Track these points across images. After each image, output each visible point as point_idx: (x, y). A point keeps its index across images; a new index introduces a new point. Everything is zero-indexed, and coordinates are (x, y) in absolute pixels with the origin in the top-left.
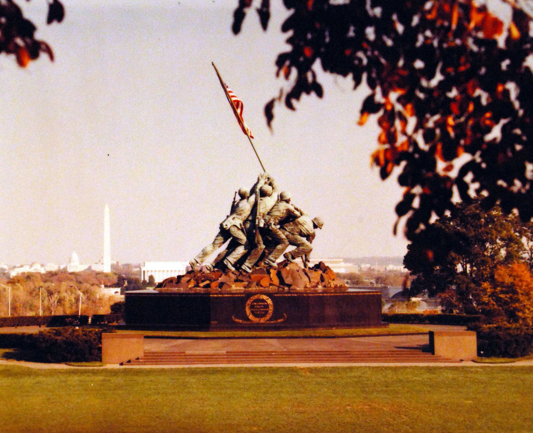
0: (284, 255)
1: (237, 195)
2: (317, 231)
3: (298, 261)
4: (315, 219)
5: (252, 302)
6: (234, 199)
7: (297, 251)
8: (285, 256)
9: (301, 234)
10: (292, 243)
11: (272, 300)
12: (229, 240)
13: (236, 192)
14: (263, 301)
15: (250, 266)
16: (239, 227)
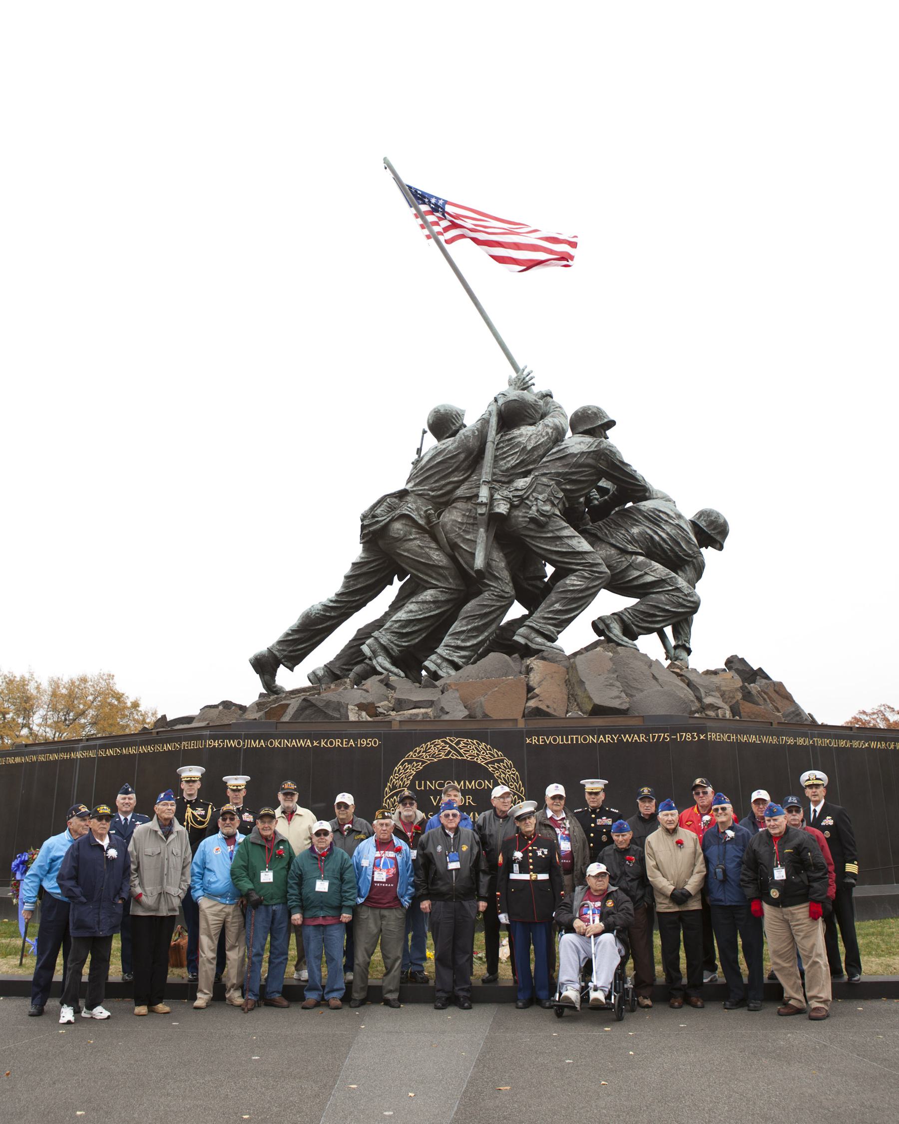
0: (594, 625)
1: (429, 436)
2: (708, 554)
3: (649, 645)
4: (701, 514)
5: (419, 776)
6: (419, 451)
7: (643, 608)
8: (599, 626)
9: (654, 551)
10: (619, 586)
11: (518, 766)
12: (397, 584)
13: (424, 432)
14: (473, 770)
15: (460, 661)
16: (422, 522)
